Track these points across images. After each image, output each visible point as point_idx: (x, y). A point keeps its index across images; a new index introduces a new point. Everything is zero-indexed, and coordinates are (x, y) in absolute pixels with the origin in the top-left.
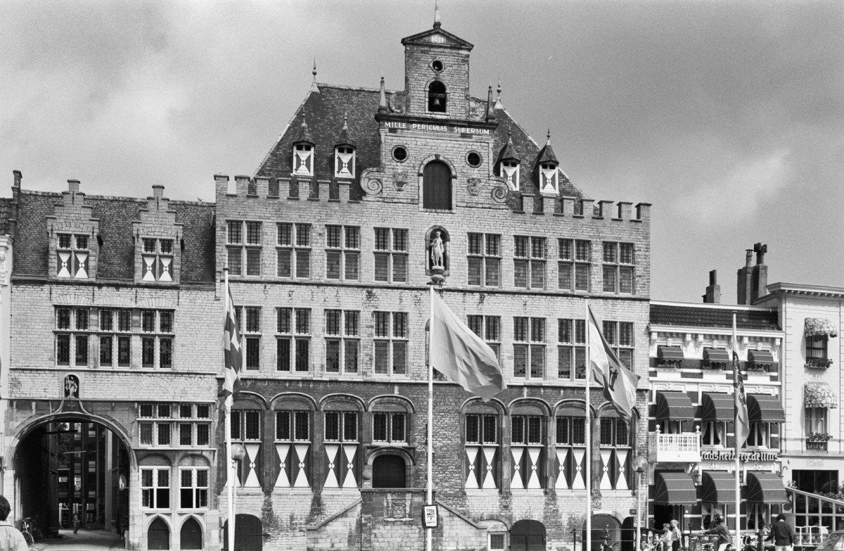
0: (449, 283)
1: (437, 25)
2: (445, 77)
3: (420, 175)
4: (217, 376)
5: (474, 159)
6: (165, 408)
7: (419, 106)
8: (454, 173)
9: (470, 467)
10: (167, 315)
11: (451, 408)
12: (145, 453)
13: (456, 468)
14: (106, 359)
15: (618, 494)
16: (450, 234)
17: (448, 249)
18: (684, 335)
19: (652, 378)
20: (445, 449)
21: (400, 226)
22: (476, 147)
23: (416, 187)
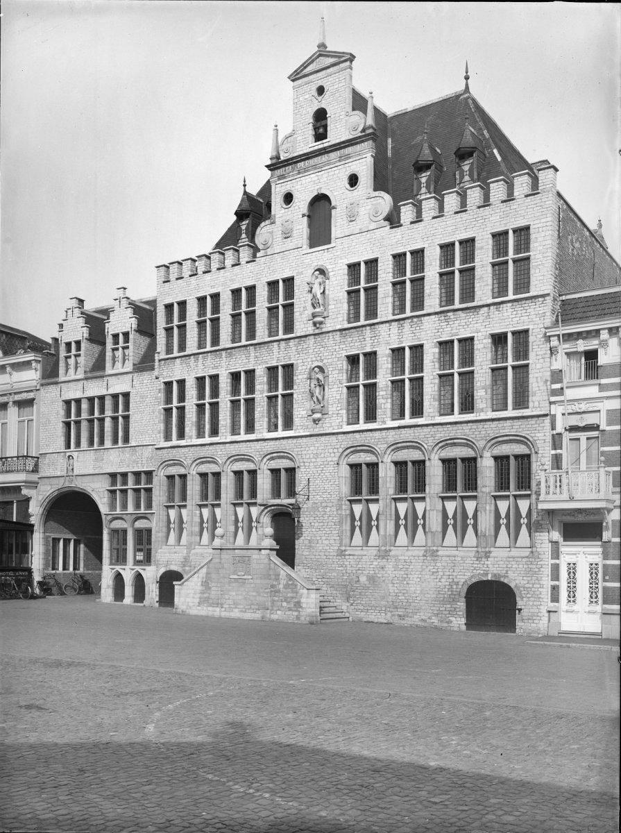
0: (328, 326)
1: (322, 45)
2: (325, 102)
3: (303, 215)
4: (156, 447)
5: (353, 180)
6: (124, 475)
7: (307, 143)
8: (333, 204)
9: (501, 521)
10: (126, 395)
11: (330, 459)
12: (135, 516)
13: (335, 525)
14: (91, 443)
15: (515, 552)
16: (329, 270)
17: (327, 288)
18: (598, 332)
19: (553, 399)
20: (323, 504)
21: (287, 275)
22: (354, 166)
23: (301, 228)
